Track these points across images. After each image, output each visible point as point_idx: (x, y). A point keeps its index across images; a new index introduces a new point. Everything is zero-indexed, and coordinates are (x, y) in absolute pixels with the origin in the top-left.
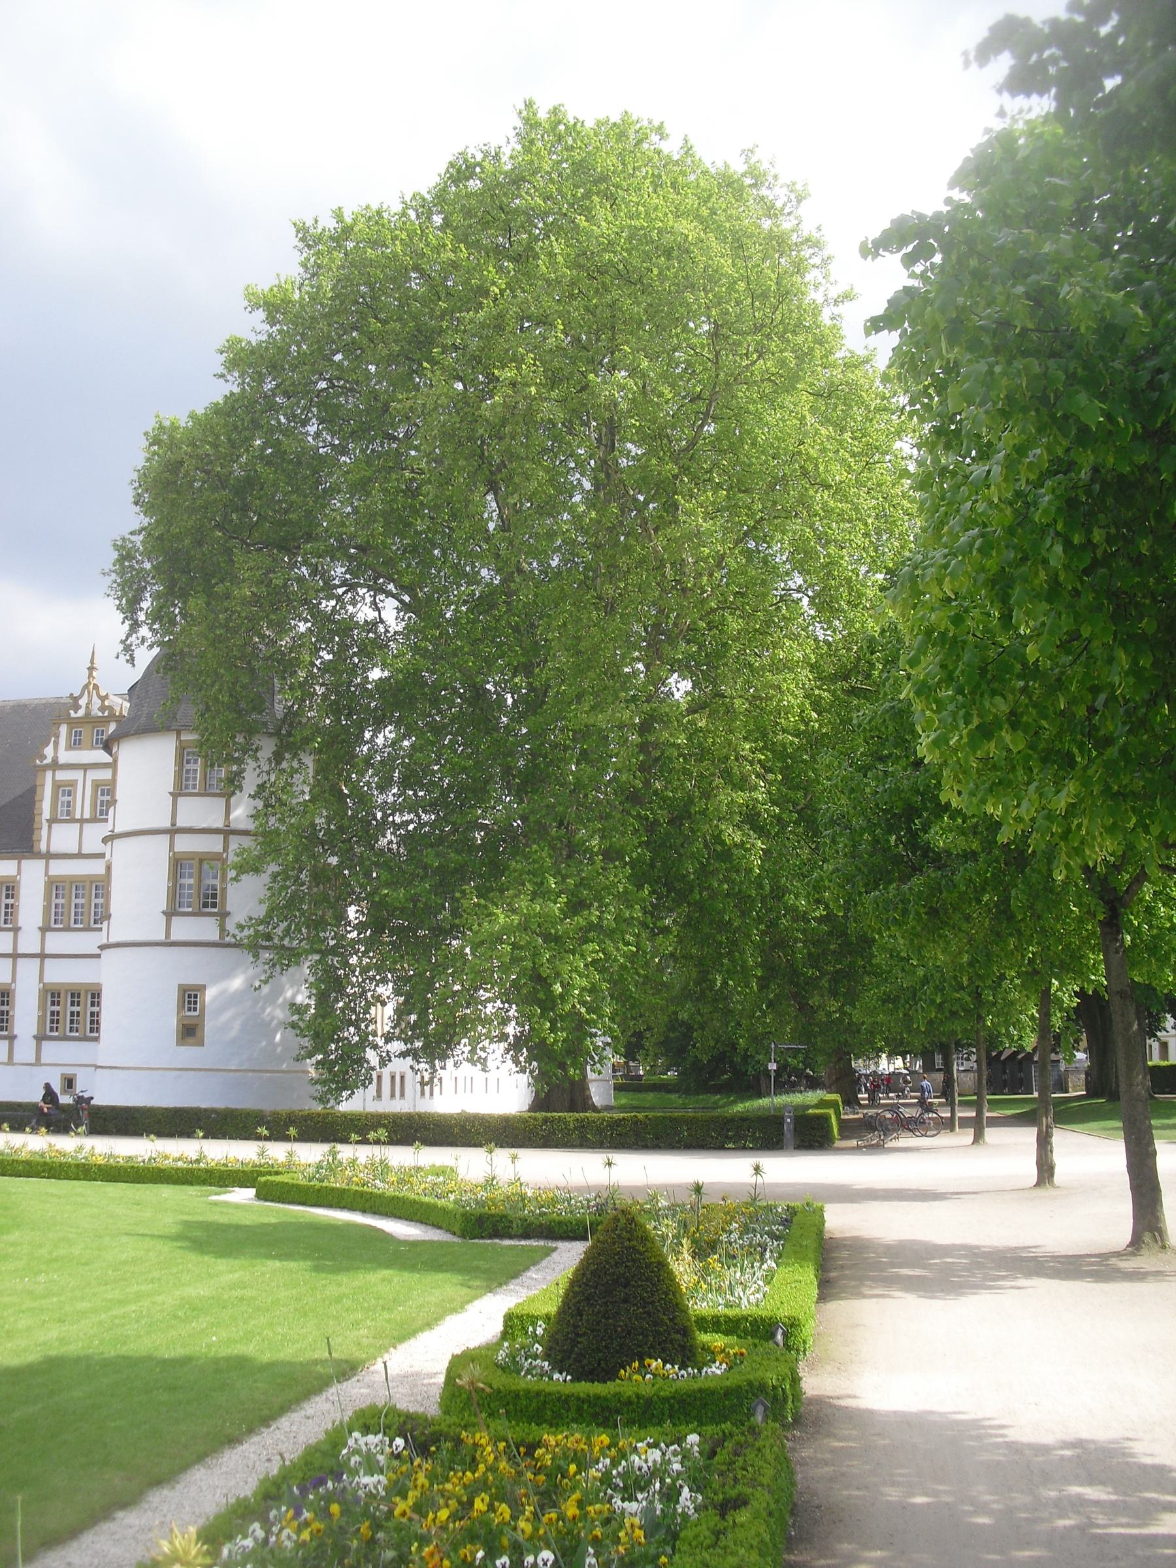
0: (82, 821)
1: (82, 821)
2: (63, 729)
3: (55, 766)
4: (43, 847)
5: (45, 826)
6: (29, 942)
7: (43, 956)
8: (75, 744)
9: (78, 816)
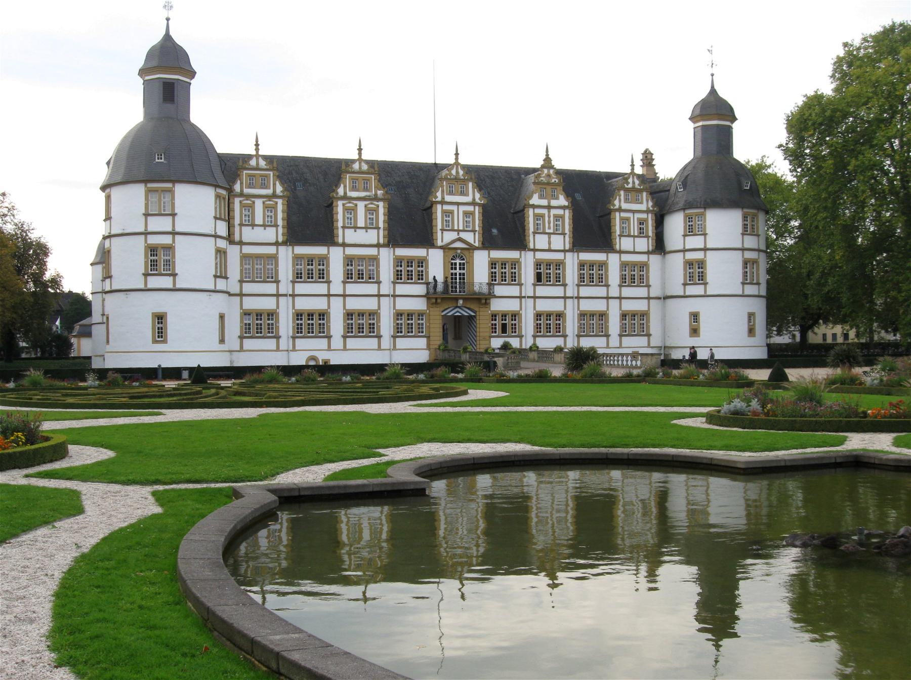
0: (634, 237)
1: (634, 237)
3: (620, 210)
4: (618, 247)
8: (627, 201)
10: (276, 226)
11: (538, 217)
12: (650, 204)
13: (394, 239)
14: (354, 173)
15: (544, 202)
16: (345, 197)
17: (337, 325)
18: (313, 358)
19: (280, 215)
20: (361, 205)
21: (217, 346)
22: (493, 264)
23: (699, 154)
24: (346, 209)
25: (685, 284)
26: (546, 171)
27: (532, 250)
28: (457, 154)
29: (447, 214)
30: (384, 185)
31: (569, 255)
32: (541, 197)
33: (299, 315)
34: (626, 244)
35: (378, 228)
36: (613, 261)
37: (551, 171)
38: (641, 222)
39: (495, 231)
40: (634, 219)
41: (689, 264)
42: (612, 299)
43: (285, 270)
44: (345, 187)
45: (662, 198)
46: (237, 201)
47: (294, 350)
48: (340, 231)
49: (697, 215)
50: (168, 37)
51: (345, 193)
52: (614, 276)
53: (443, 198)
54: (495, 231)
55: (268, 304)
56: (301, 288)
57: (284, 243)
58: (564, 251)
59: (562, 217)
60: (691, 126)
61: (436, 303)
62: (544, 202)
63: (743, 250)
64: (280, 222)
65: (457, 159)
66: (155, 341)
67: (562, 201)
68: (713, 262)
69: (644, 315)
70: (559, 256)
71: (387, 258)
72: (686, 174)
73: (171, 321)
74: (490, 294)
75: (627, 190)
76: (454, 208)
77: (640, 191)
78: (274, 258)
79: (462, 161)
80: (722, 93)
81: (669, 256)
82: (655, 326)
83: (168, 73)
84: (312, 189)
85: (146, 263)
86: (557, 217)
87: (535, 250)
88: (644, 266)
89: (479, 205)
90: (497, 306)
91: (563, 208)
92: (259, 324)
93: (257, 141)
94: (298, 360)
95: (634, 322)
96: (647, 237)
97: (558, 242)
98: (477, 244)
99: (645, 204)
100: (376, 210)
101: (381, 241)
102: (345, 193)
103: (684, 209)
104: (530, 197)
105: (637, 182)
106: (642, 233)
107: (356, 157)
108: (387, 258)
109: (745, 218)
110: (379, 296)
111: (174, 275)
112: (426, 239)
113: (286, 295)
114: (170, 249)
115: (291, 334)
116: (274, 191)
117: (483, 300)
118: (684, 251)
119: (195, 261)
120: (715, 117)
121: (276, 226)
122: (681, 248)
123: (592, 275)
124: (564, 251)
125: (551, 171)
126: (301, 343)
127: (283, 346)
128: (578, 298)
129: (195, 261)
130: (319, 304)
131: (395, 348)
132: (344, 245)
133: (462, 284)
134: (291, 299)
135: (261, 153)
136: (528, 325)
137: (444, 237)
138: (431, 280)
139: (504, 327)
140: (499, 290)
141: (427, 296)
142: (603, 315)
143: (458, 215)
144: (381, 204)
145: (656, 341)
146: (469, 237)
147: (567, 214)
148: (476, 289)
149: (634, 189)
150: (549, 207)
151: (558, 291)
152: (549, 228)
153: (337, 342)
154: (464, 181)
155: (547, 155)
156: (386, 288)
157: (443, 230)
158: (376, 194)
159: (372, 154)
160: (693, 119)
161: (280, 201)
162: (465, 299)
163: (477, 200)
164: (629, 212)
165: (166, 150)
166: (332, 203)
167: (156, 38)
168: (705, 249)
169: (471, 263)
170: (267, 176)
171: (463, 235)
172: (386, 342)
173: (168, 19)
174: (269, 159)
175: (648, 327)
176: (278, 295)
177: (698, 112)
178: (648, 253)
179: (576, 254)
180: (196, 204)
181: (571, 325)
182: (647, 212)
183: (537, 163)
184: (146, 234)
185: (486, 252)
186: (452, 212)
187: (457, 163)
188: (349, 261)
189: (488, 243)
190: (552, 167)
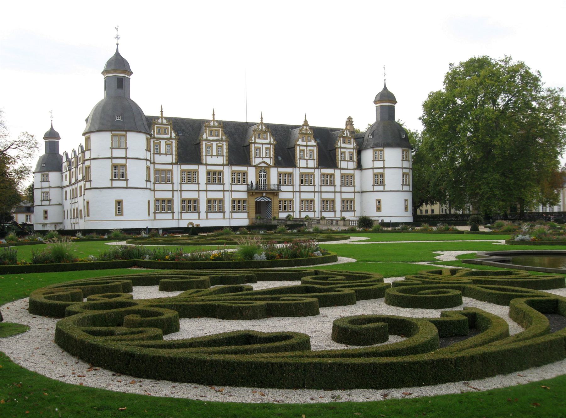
0: (347, 161)
1: (347, 161)
2: (341, 139)
3: (341, 147)
4: (339, 166)
8: (344, 143)
10: (172, 154)
11: (301, 151)
12: (355, 144)
13: (231, 162)
14: (211, 127)
15: (304, 143)
16: (206, 140)
17: (203, 206)
18: (191, 224)
19: (174, 149)
20: (215, 144)
21: (147, 217)
22: (280, 175)
23: (379, 119)
24: (208, 147)
25: (373, 185)
26: (305, 127)
28: (262, 118)
29: (257, 149)
30: (225, 133)
31: (316, 170)
32: (303, 140)
33: (183, 201)
34: (343, 165)
35: (223, 156)
36: (338, 174)
37: (308, 128)
38: (351, 154)
39: (280, 158)
40: (347, 152)
41: (376, 175)
42: (337, 193)
43: (177, 177)
44: (206, 134)
45: (361, 142)
46: (152, 141)
47: (181, 219)
48: (204, 157)
49: (380, 150)
50: (117, 54)
51: (207, 138)
53: (255, 141)
54: (280, 158)
55: (168, 195)
56: (185, 187)
57: (176, 163)
58: (314, 168)
59: (313, 151)
60: (374, 106)
61: (253, 195)
62: (304, 143)
63: (402, 168)
64: (174, 152)
65: (262, 120)
66: (117, 215)
67: (313, 143)
68: (388, 174)
69: (352, 201)
70: (311, 171)
71: (227, 171)
72: (373, 130)
73: (125, 204)
74: (278, 189)
75: (344, 138)
76: (261, 146)
77: (351, 138)
78: (171, 171)
79: (265, 121)
80: (390, 89)
81: (365, 172)
82: (357, 207)
83: (118, 72)
84: (186, 135)
85: (112, 173)
86: (310, 151)
87: (300, 168)
88: (352, 176)
89: (273, 144)
90: (282, 196)
91: (314, 146)
92: (163, 206)
93: (162, 109)
94: (184, 224)
95: (348, 204)
96: (353, 161)
98: (272, 165)
99: (353, 144)
100: (222, 147)
101: (225, 163)
102: (207, 138)
103: (373, 148)
104: (298, 141)
105: (348, 134)
106: (351, 159)
107: (212, 119)
108: (227, 171)
109: (403, 152)
110: (224, 191)
111: (127, 180)
112: (247, 162)
113: (177, 191)
114: (124, 166)
115: (180, 211)
116: (171, 136)
117: (275, 193)
118: (373, 168)
119: (137, 173)
120: (386, 100)
121: (172, 154)
122: (372, 167)
123: (328, 180)
124: (314, 168)
125: (308, 128)
126: (185, 216)
127: (176, 217)
128: (321, 192)
129: (137, 173)
130: (194, 195)
131: (232, 218)
132: (206, 165)
133: (265, 184)
134: (179, 192)
135: (164, 116)
136: (297, 206)
137: (256, 161)
138: (249, 183)
139: (285, 207)
140: (283, 188)
141: (248, 191)
142: (333, 201)
143: (262, 149)
144: (224, 143)
145: (358, 214)
146: (268, 161)
147: (316, 149)
148: (272, 187)
149: (347, 137)
150: (307, 146)
151: (311, 189)
153: (203, 215)
154: (265, 132)
155: (306, 119)
156: (227, 187)
157: (255, 157)
158: (222, 138)
159: (220, 117)
160: (375, 102)
161: (174, 141)
162: (267, 193)
163: (272, 142)
164: (346, 148)
165: (118, 114)
166: (200, 143)
167: (112, 54)
168: (384, 168)
169: (269, 174)
170: (167, 128)
171: (265, 160)
172: (227, 215)
173: (117, 44)
174: (168, 119)
175: (354, 207)
176: (173, 191)
177: (378, 99)
178: (354, 169)
180: (136, 142)
181: (318, 206)
182: (353, 148)
183: (301, 123)
184: (111, 158)
185: (276, 169)
186: (259, 148)
187: (262, 123)
188: (208, 173)
189: (277, 164)
190: (308, 125)
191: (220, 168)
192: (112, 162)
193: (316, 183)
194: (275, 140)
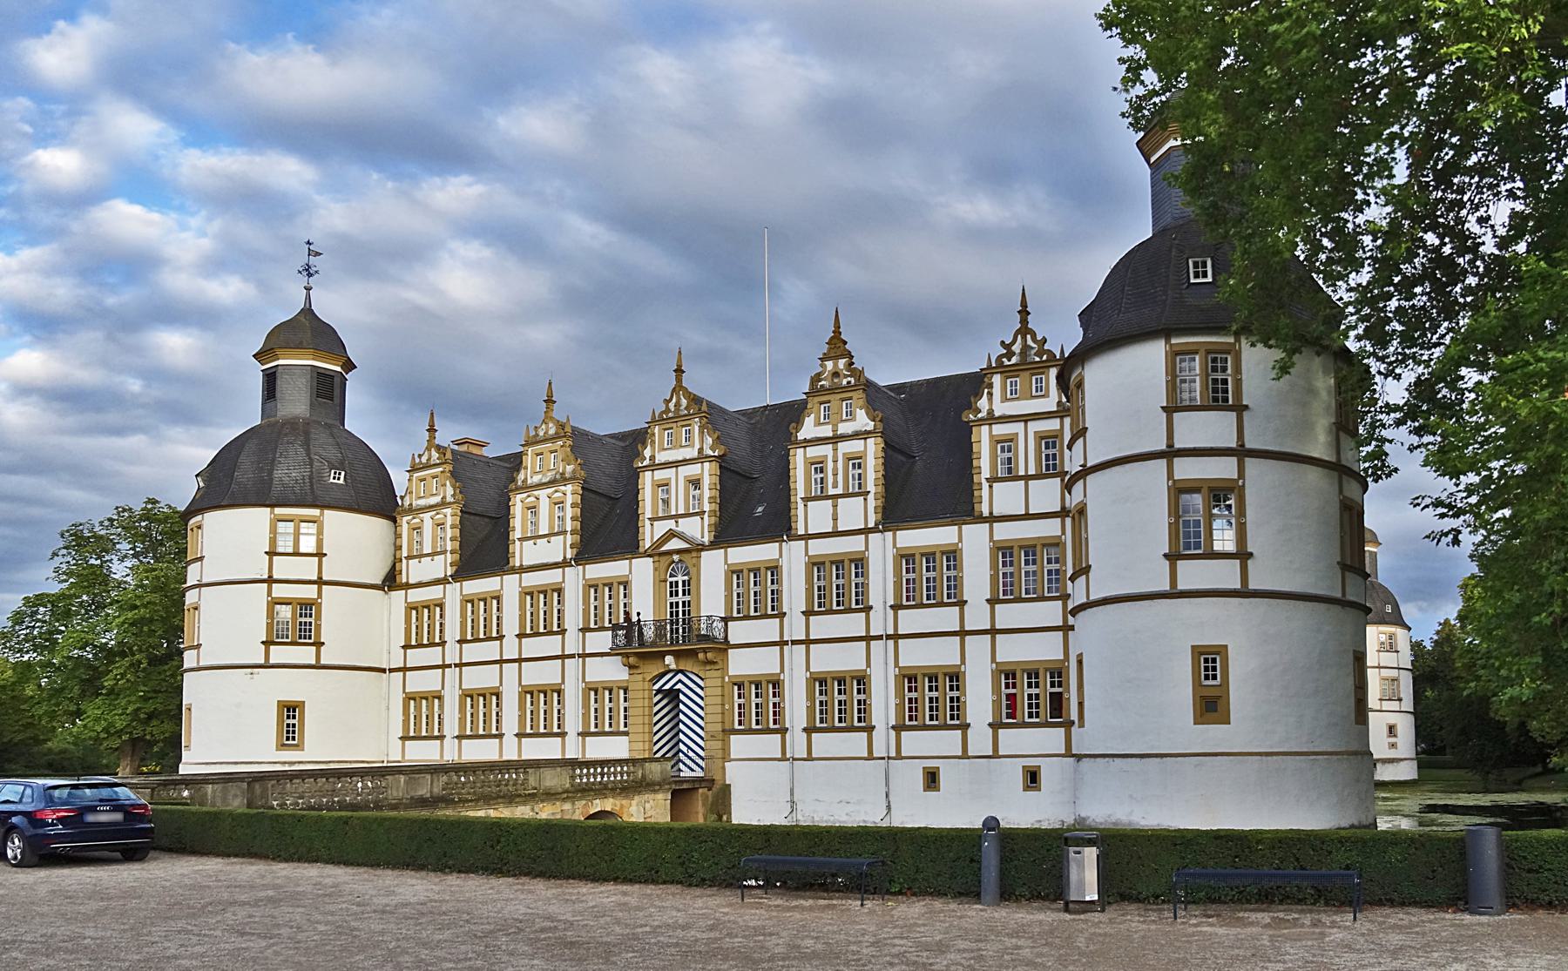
0: (1027, 478)
1: (1027, 478)
3: (992, 419)
5: (985, 485)
6: (977, 616)
7: (993, 632)
9: (1022, 473)
15: (826, 431)
26: (829, 365)
27: (801, 538)
52: (977, 577)
53: (652, 458)
67: (863, 421)
87: (807, 537)
90: (740, 664)
97: (855, 513)
104: (799, 423)
123: (929, 582)
133: (688, 622)
137: (650, 533)
147: (872, 450)
152: (835, 486)
164: (1010, 417)
179: (889, 535)
191: (553, 577)
192: (269, 594)
193: (875, 598)
194: (718, 441)
